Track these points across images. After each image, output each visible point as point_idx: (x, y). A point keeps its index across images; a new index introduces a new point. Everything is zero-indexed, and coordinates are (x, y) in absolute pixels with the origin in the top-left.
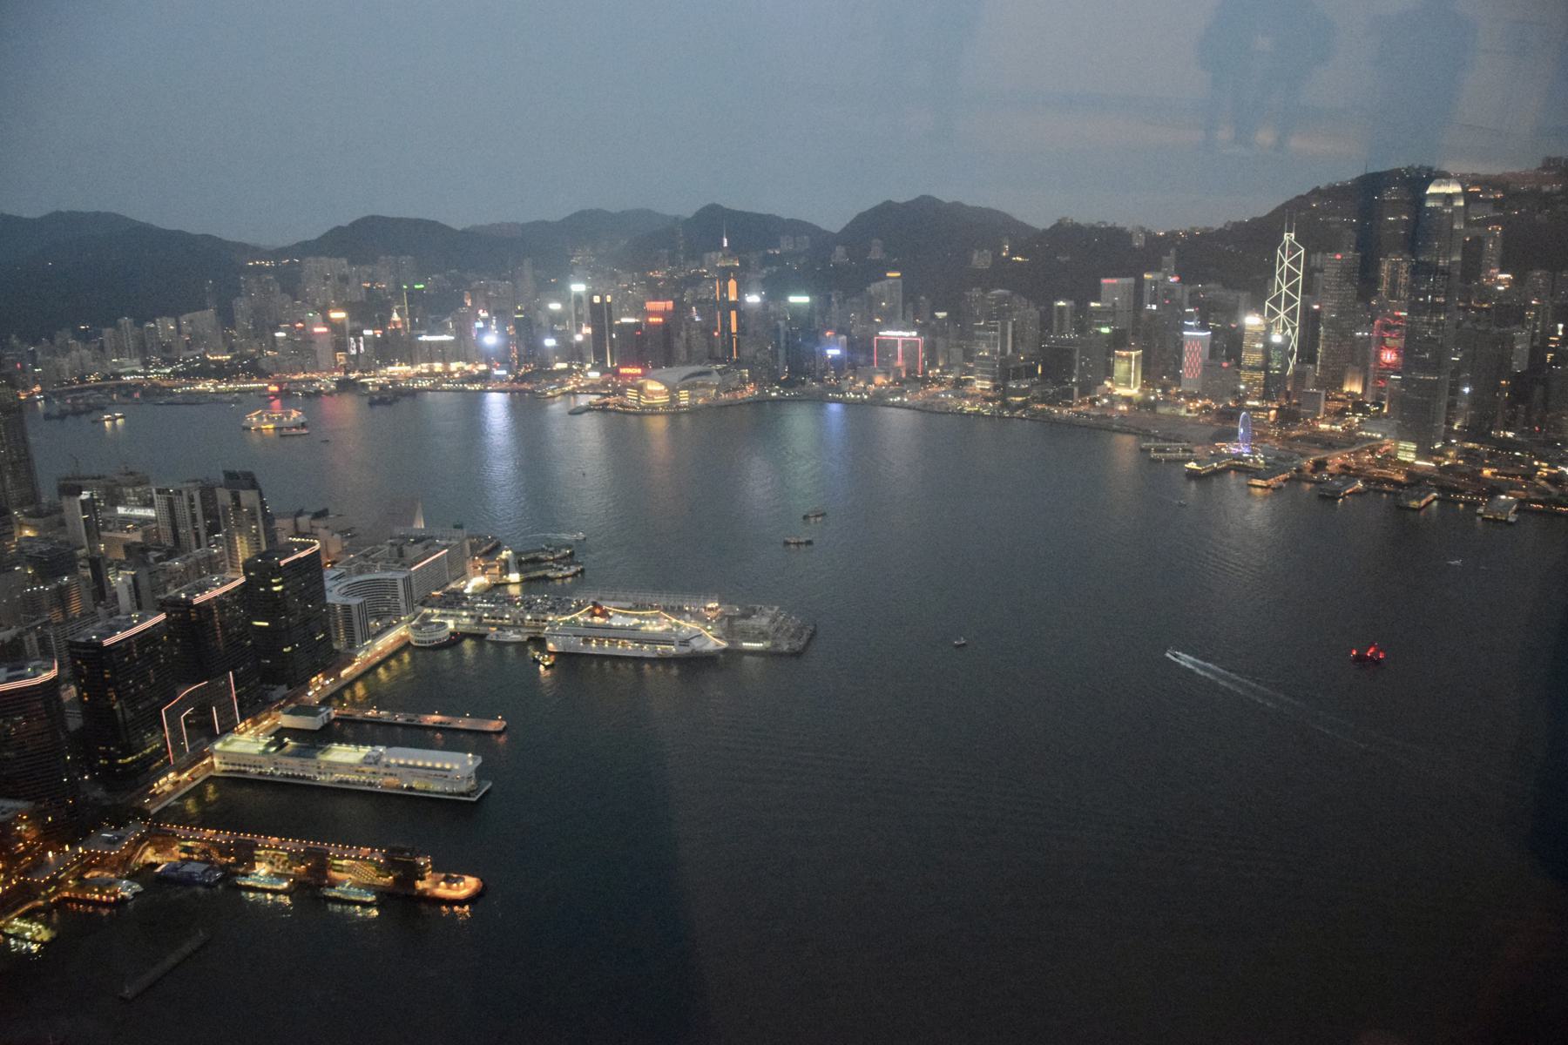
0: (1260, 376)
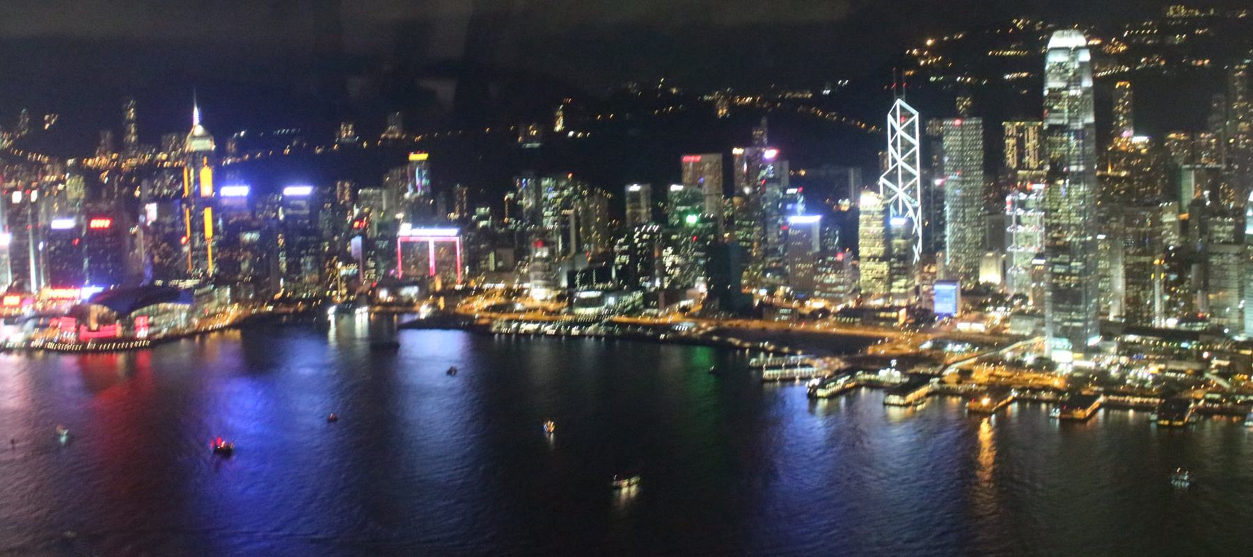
0: (884, 267)
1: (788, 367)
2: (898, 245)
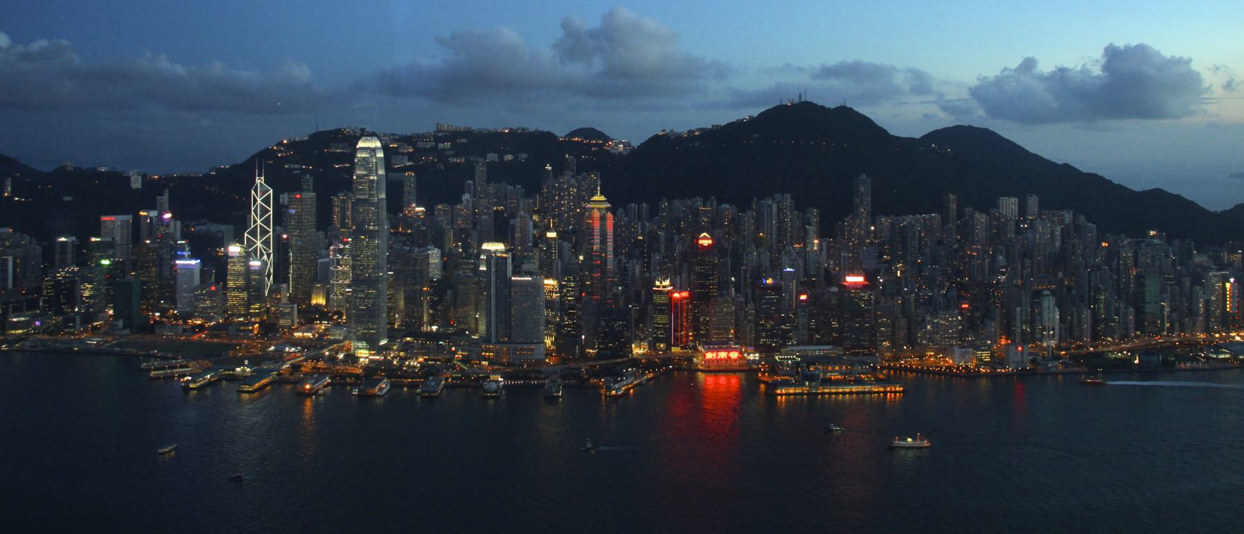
0: (244, 295)
1: (170, 368)
2: (255, 279)
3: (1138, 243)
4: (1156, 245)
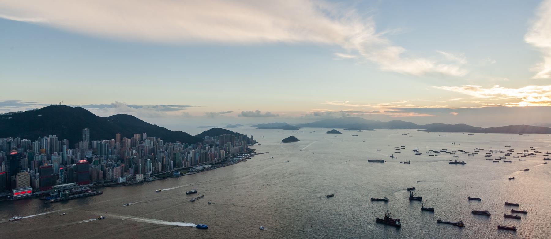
3: (174, 145)
4: (179, 145)
